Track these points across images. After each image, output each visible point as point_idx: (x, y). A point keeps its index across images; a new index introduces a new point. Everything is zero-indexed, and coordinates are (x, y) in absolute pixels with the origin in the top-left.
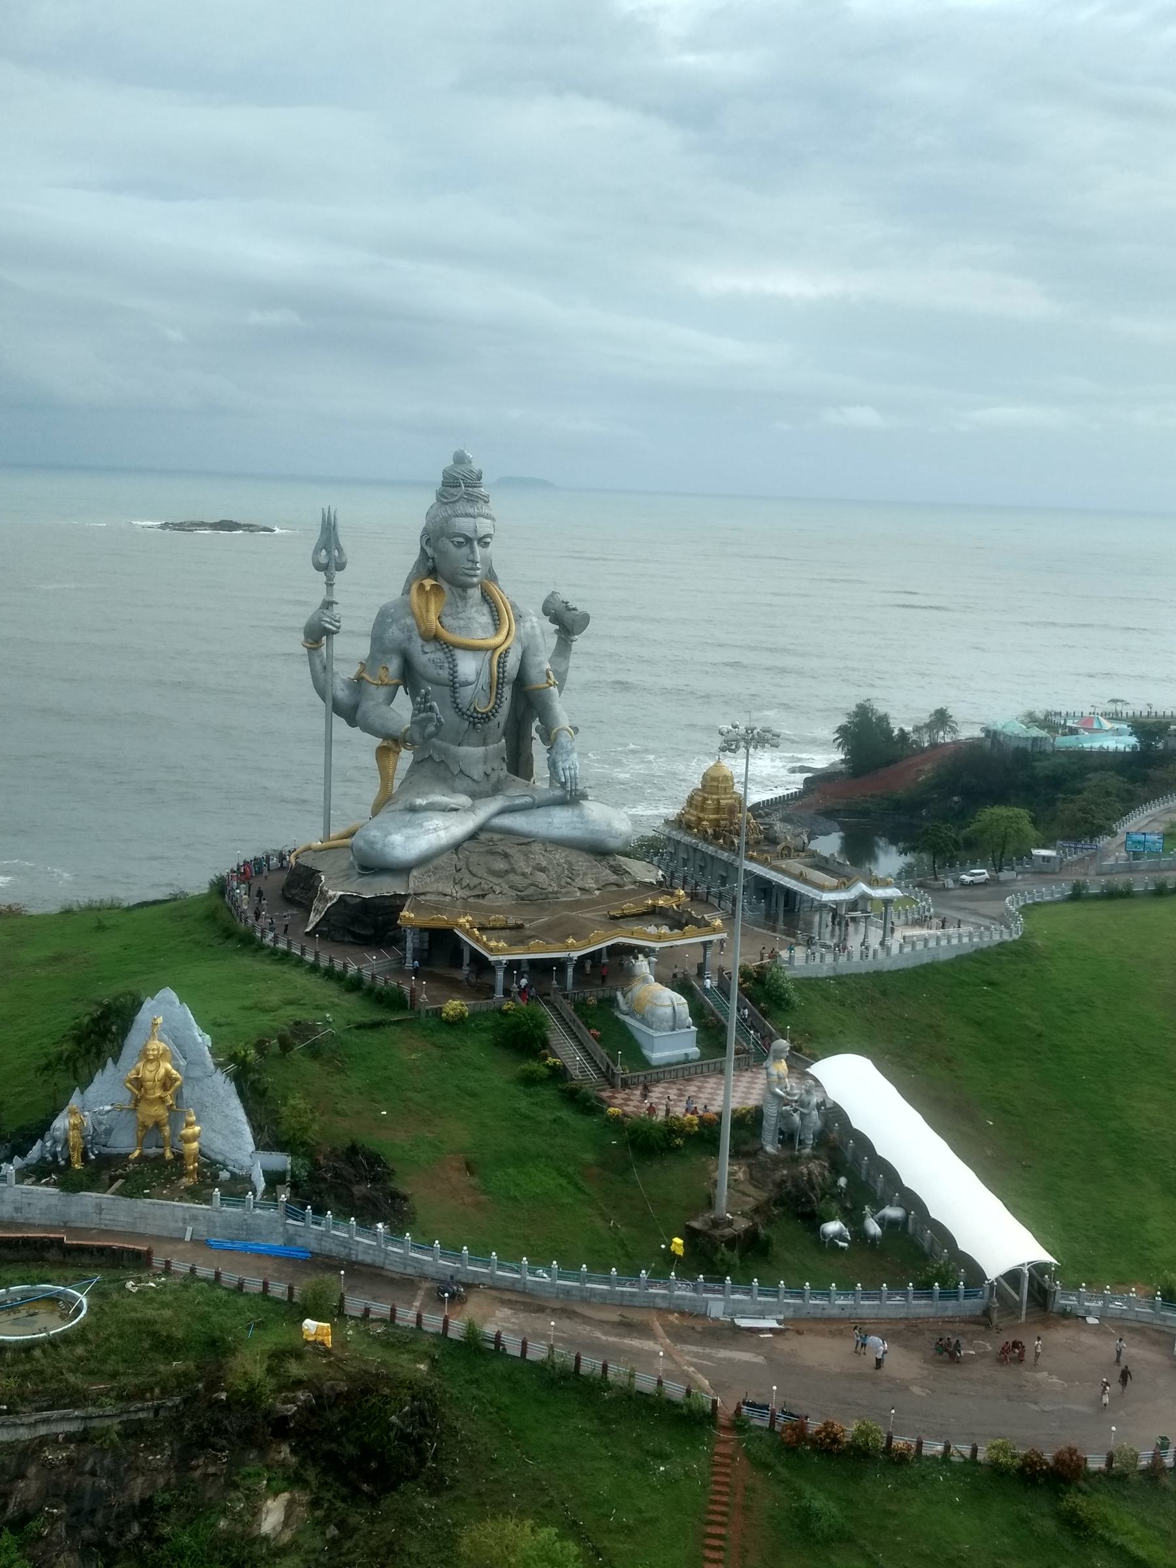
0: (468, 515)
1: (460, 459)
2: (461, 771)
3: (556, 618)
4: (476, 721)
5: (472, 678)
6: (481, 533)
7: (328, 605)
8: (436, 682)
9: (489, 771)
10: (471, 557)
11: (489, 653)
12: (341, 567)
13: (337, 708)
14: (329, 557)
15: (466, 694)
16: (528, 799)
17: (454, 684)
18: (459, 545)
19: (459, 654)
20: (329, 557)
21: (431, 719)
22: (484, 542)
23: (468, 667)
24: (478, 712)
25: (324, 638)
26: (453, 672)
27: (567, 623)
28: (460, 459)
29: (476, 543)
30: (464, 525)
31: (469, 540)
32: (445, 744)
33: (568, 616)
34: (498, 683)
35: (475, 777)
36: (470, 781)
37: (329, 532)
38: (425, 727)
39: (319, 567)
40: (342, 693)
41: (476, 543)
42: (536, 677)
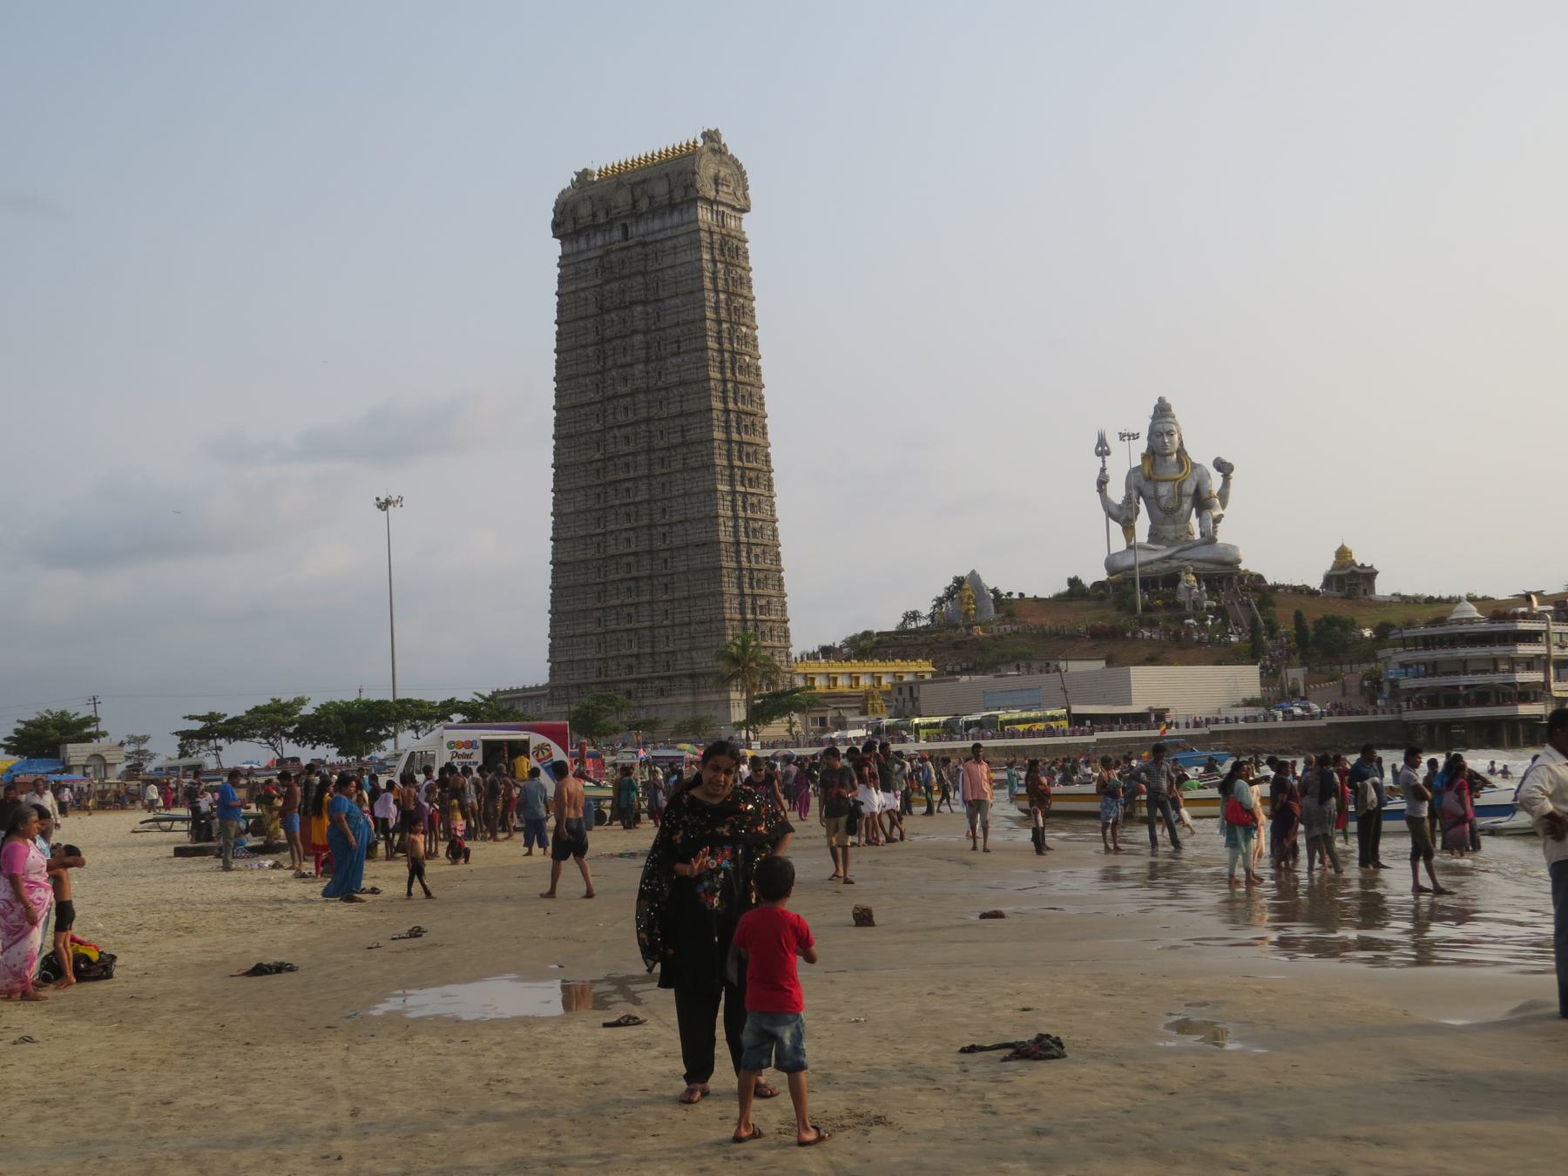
1: (1161, 400)
7: (1103, 470)
12: (1108, 453)
13: (1110, 515)
14: (1102, 450)
15: (1163, 501)
17: (1157, 498)
20: (1102, 450)
22: (1170, 434)
23: (1164, 489)
27: (1224, 467)
28: (1161, 400)
30: (1159, 427)
37: (1102, 441)
39: (1098, 454)
40: (1114, 510)
42: (1205, 495)
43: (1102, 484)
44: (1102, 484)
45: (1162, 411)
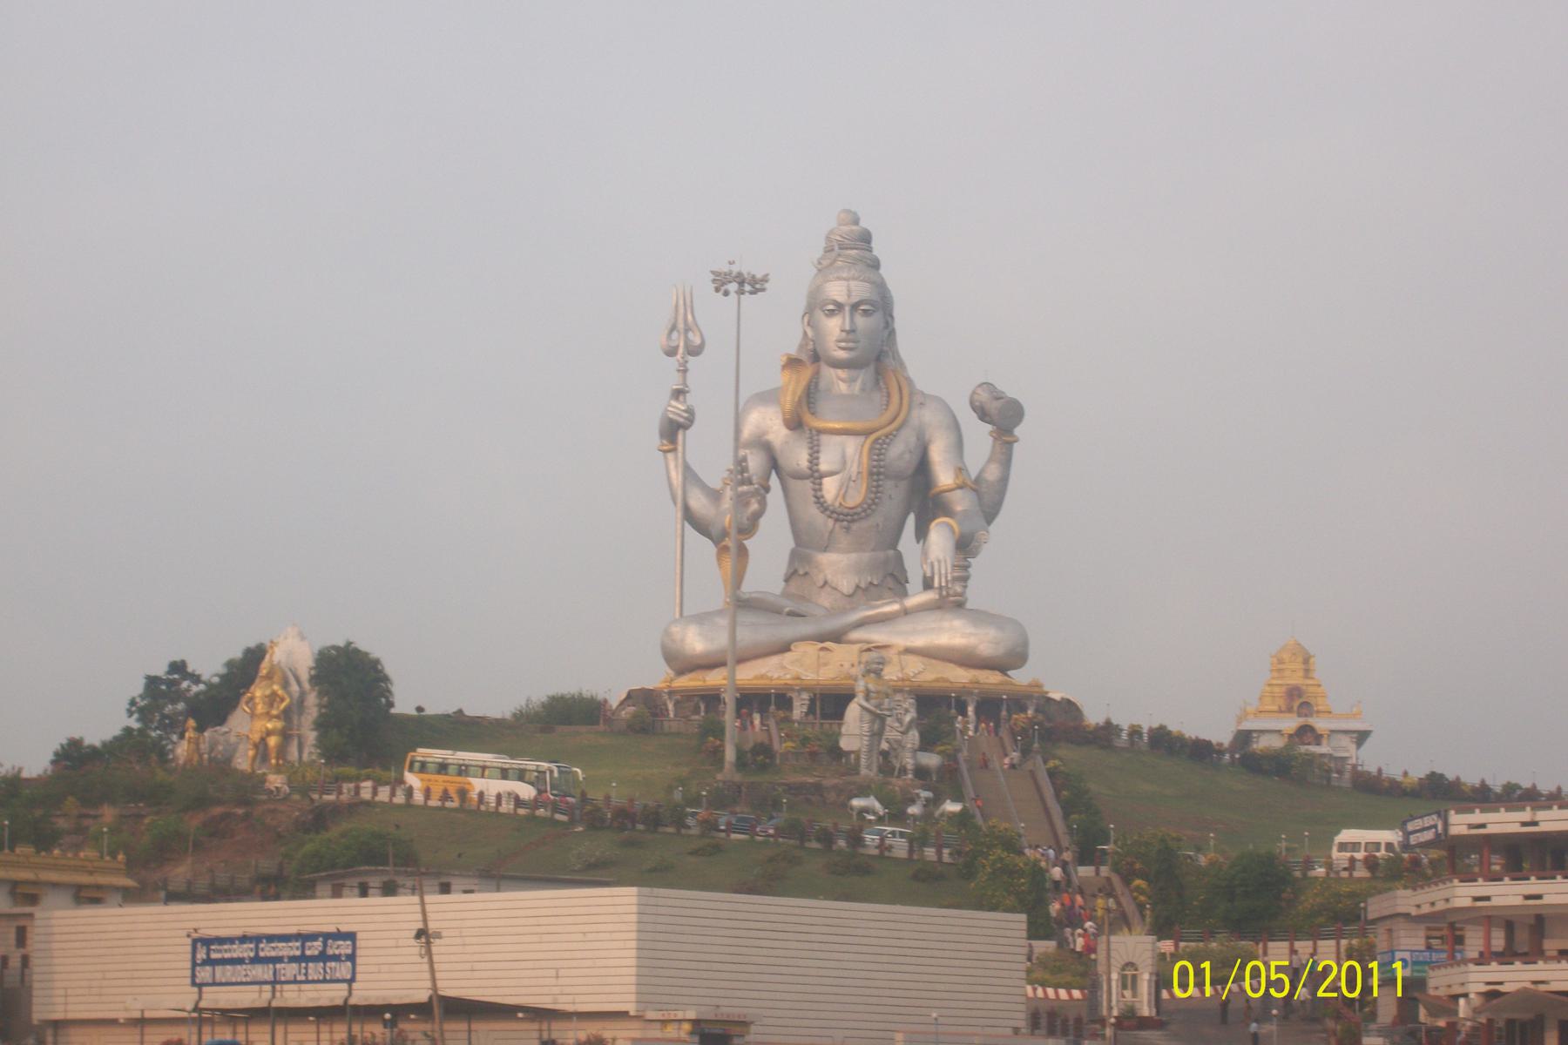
0: (839, 279)
2: (826, 583)
3: (983, 414)
4: (845, 517)
6: (855, 300)
8: (799, 476)
9: (863, 585)
11: (862, 439)
16: (896, 607)
17: (815, 476)
18: (831, 313)
19: (824, 438)
25: (680, 437)
26: (814, 460)
29: (847, 309)
31: (839, 307)
33: (993, 407)
34: (871, 474)
35: (845, 591)
38: (747, 504)
39: (671, 352)
42: (944, 477)
43: (672, 431)
44: (672, 431)
45: (855, 247)
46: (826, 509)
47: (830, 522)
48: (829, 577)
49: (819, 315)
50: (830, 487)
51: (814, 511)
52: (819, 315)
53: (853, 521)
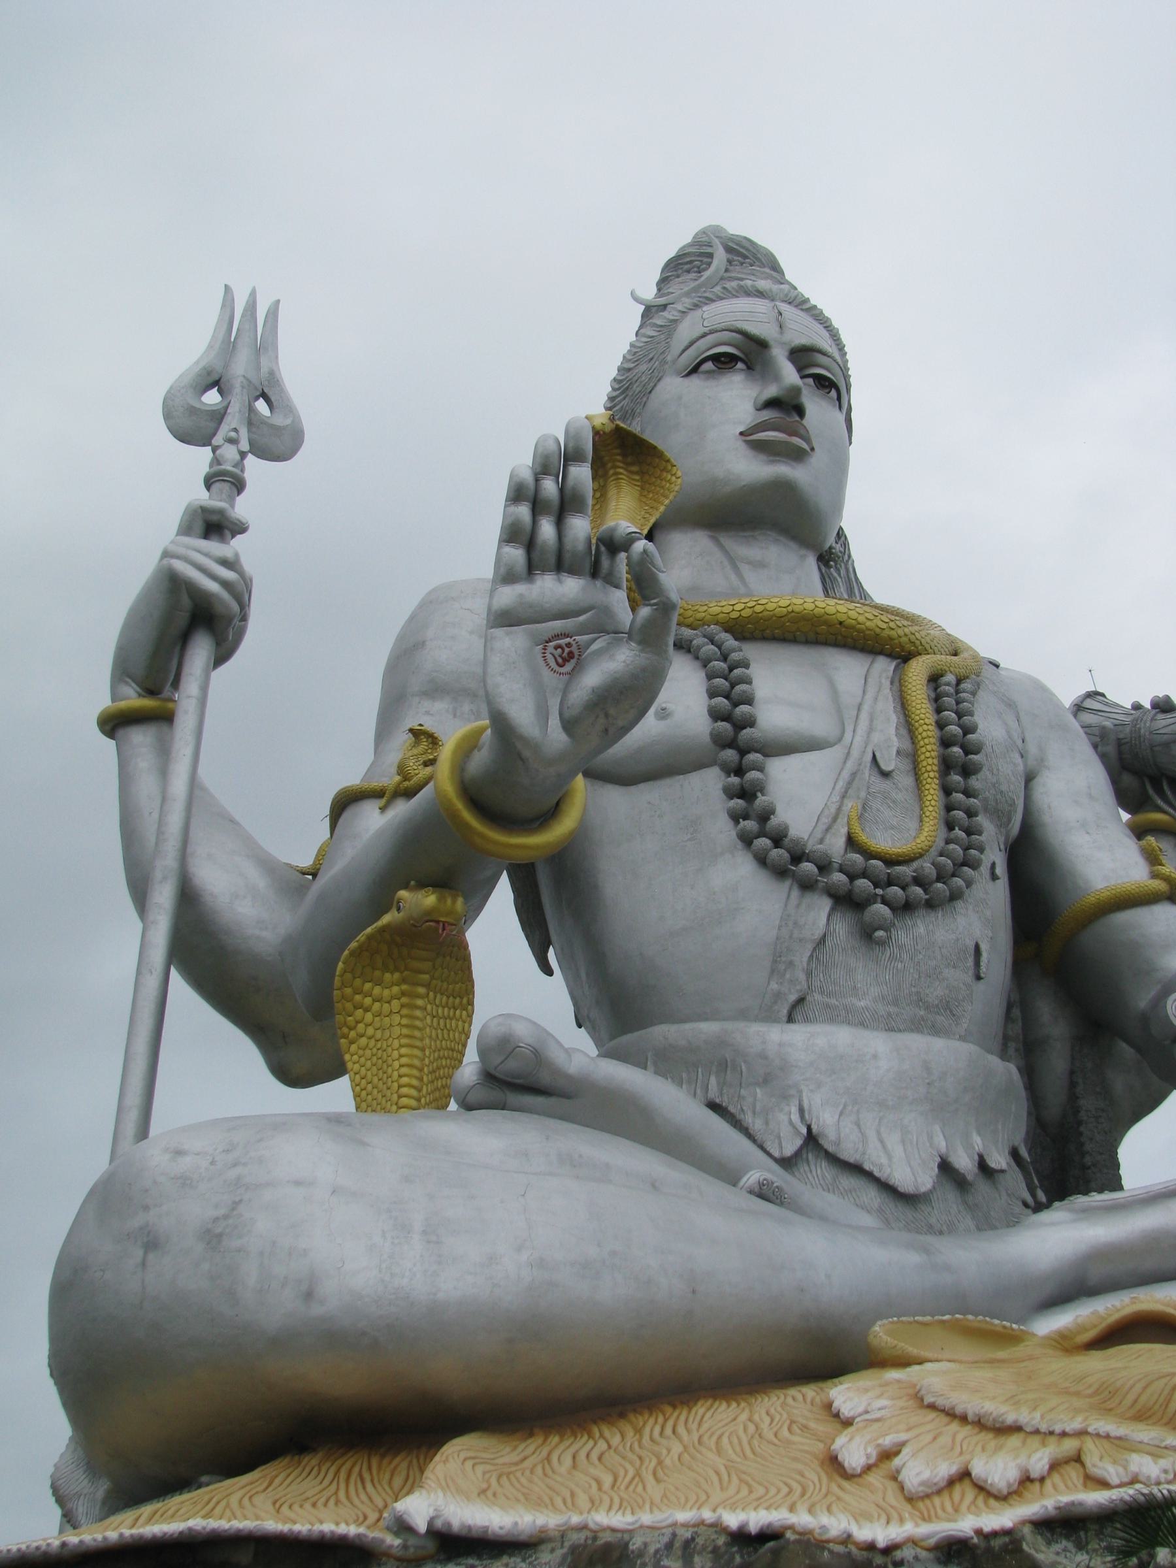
2: (812, 1140)
4: (868, 893)
5: (818, 725)
9: (964, 1163)
10: (772, 391)
11: (884, 667)
17: (737, 747)
18: (723, 362)
21: (603, 626)
24: (869, 855)
32: (709, 1028)
34: (947, 765)
36: (871, 1195)
38: (569, 658)
39: (192, 427)
41: (780, 356)
46: (798, 857)
47: (817, 913)
48: (826, 1120)
49: (673, 387)
50: (801, 795)
51: (738, 873)
52: (673, 387)
53: (906, 908)
